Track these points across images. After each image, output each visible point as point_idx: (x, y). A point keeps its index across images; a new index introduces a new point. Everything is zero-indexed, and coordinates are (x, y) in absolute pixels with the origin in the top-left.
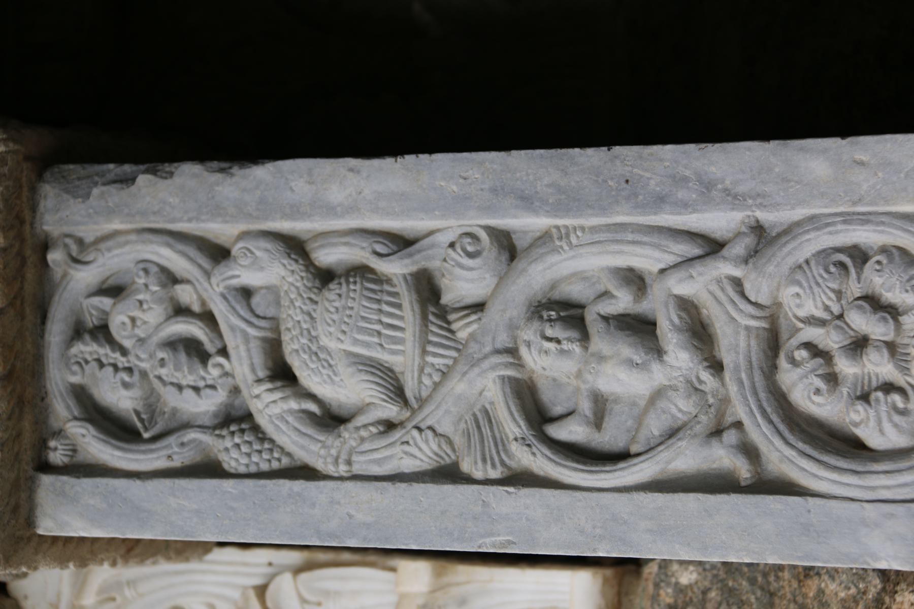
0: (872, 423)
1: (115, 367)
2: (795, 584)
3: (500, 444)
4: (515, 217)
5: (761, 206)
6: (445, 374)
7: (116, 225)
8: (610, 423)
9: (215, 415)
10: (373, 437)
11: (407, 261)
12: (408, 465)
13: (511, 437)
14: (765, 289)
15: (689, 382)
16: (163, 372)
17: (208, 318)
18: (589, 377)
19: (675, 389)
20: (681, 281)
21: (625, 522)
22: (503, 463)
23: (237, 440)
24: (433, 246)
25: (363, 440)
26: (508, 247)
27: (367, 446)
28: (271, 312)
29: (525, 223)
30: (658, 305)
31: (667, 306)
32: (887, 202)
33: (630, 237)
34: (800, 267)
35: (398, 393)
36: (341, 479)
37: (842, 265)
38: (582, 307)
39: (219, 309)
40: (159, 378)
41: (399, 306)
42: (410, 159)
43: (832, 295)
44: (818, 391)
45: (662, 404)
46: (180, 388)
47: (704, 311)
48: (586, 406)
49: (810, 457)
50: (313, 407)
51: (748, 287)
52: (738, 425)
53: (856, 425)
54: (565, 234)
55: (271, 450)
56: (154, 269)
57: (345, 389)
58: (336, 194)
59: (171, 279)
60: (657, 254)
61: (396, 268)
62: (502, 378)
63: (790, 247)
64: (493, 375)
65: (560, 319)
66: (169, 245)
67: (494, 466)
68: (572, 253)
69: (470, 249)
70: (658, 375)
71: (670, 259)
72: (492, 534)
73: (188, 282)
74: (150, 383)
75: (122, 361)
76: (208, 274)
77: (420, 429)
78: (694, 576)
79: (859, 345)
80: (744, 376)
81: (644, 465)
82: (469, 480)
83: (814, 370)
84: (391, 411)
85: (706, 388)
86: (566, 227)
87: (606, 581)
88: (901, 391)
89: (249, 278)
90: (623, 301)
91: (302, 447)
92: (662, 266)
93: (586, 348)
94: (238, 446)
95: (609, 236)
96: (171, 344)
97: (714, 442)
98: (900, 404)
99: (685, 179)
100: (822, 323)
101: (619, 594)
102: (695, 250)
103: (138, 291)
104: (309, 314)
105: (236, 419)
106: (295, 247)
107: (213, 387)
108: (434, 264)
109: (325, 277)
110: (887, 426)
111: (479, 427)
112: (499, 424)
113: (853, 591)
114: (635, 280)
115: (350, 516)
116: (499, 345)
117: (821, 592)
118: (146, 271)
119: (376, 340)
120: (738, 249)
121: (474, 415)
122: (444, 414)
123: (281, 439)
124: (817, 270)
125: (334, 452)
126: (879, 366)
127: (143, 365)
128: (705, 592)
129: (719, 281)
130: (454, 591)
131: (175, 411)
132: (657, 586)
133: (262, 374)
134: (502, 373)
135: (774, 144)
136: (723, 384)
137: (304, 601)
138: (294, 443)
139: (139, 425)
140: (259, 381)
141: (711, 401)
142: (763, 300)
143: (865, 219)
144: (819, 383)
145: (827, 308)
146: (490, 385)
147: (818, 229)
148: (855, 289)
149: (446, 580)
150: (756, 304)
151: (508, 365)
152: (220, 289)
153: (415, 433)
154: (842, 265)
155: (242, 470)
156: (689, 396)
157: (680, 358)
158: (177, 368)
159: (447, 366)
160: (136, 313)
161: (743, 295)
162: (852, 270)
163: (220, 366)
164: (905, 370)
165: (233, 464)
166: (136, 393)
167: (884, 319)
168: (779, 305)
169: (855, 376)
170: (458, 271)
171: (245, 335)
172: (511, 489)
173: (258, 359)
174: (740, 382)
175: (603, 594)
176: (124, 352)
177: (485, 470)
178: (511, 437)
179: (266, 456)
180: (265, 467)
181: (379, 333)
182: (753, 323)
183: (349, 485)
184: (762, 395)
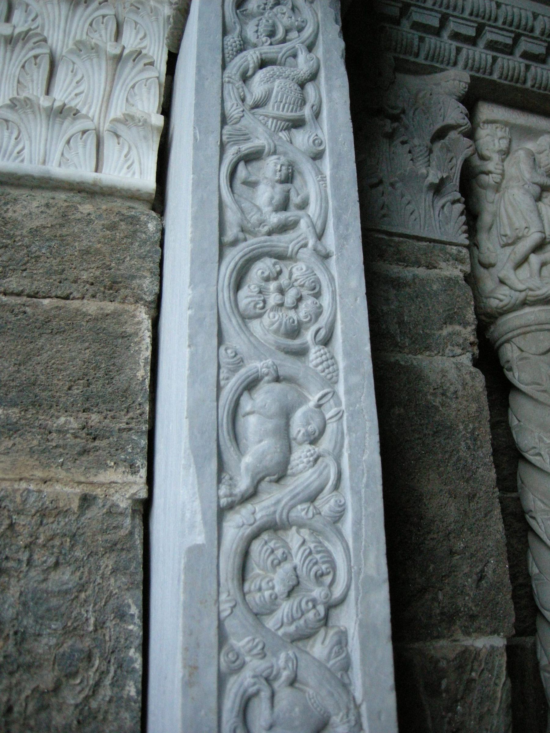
0: (250, 294)
1: (266, 4)
2: (148, 268)
3: (236, 142)
4: (330, 161)
5: (338, 259)
6: (265, 124)
7: (320, 15)
8: (245, 188)
9: (246, 37)
10: (239, 94)
11: (310, 117)
12: (228, 105)
13: (241, 147)
14: (305, 256)
15: (264, 222)
16: (264, 21)
17: (284, 41)
18: (265, 181)
19: (261, 215)
20: (307, 223)
21: (206, 187)
22: (228, 142)
23: (237, 42)
24: (316, 128)
25: (238, 89)
26: (317, 156)
27: (235, 90)
28: (287, 64)
29: (327, 165)
30: (291, 214)
31: (296, 216)
32: (341, 309)
33: (323, 205)
34: (313, 272)
35: (257, 106)
36: (222, 78)
37: (314, 289)
38: (292, 183)
39: (288, 45)
40: (261, 19)
41: (292, 111)
42: (351, 125)
43: (302, 283)
44: (263, 273)
45: (255, 210)
46: (258, 25)
47: (291, 232)
48: (253, 178)
49: (235, 266)
50: (250, 73)
51: (305, 249)
52: (245, 240)
53: (249, 287)
54: (324, 179)
55: (233, 55)
56: (304, 25)
57: (258, 85)
58: (336, 95)
59: (300, 30)
60: (316, 215)
61: (307, 112)
62: (264, 147)
63: (322, 268)
64: (266, 143)
65: (289, 173)
66: (313, 31)
67: (228, 138)
68: (316, 181)
69: (317, 142)
70: (267, 209)
71: (315, 220)
72: (200, 132)
73: (299, 36)
74: (259, 16)
75: (268, 7)
76: (303, 43)
77: (243, 111)
78: (151, 230)
79: (282, 291)
80: (269, 243)
81: (230, 198)
82: (222, 128)
83: (271, 272)
84: (250, 101)
85: (260, 228)
86: (326, 180)
87: (151, 194)
88: (264, 307)
89: (302, 57)
90: (295, 199)
91: (234, 66)
92: (311, 216)
93: (277, 182)
94: (235, 42)
95: (323, 197)
96: (274, 26)
97: (239, 229)
98: (258, 306)
99: (347, 230)
100: (290, 278)
101: (144, 200)
102: (318, 231)
103: (295, 17)
104: (288, 77)
105: (244, 45)
106: (314, 77)
107: (258, 37)
108: (307, 127)
109: (302, 85)
110: (249, 299)
111: (243, 135)
112: (245, 143)
113: (146, 290)
114: (304, 205)
115: (207, 79)
116: (278, 147)
117: (145, 277)
118: (303, 22)
119: (279, 100)
120: (320, 248)
121: (248, 134)
122: (248, 121)
123: (237, 59)
124: (313, 278)
125: (233, 77)
126: (273, 299)
127: (266, 15)
128: (144, 232)
129: (306, 238)
130: (150, 135)
131: (246, 24)
132: (148, 215)
133: (264, 56)
134: (267, 147)
135: (362, 267)
136: (263, 235)
137: (147, 79)
138: (236, 63)
139: (242, 10)
140: (261, 54)
141: (257, 229)
142: (300, 255)
143: (334, 299)
144: (266, 274)
145: (296, 280)
146: (261, 142)
147: (330, 280)
148: (305, 292)
149: (155, 132)
150: (297, 252)
151: (270, 149)
152: (297, 46)
153: (241, 109)
154: (314, 289)
155: (225, 42)
156: (258, 220)
157: (274, 219)
158: (265, 26)
159: (267, 126)
160: (287, 15)
161: (301, 247)
162: (312, 292)
163: (266, 42)
164: (272, 309)
165: (228, 39)
166: (255, 10)
167: (293, 303)
168: (296, 262)
169: (269, 289)
170: (307, 136)
171: (279, 52)
172: (219, 143)
173: (270, 56)
174: (265, 242)
175: (147, 193)
176: (272, 8)
177: (226, 135)
178: (241, 147)
179: (231, 52)
180: (226, 51)
181: (281, 102)
182: (290, 249)
183: (220, 81)
184: (260, 250)
